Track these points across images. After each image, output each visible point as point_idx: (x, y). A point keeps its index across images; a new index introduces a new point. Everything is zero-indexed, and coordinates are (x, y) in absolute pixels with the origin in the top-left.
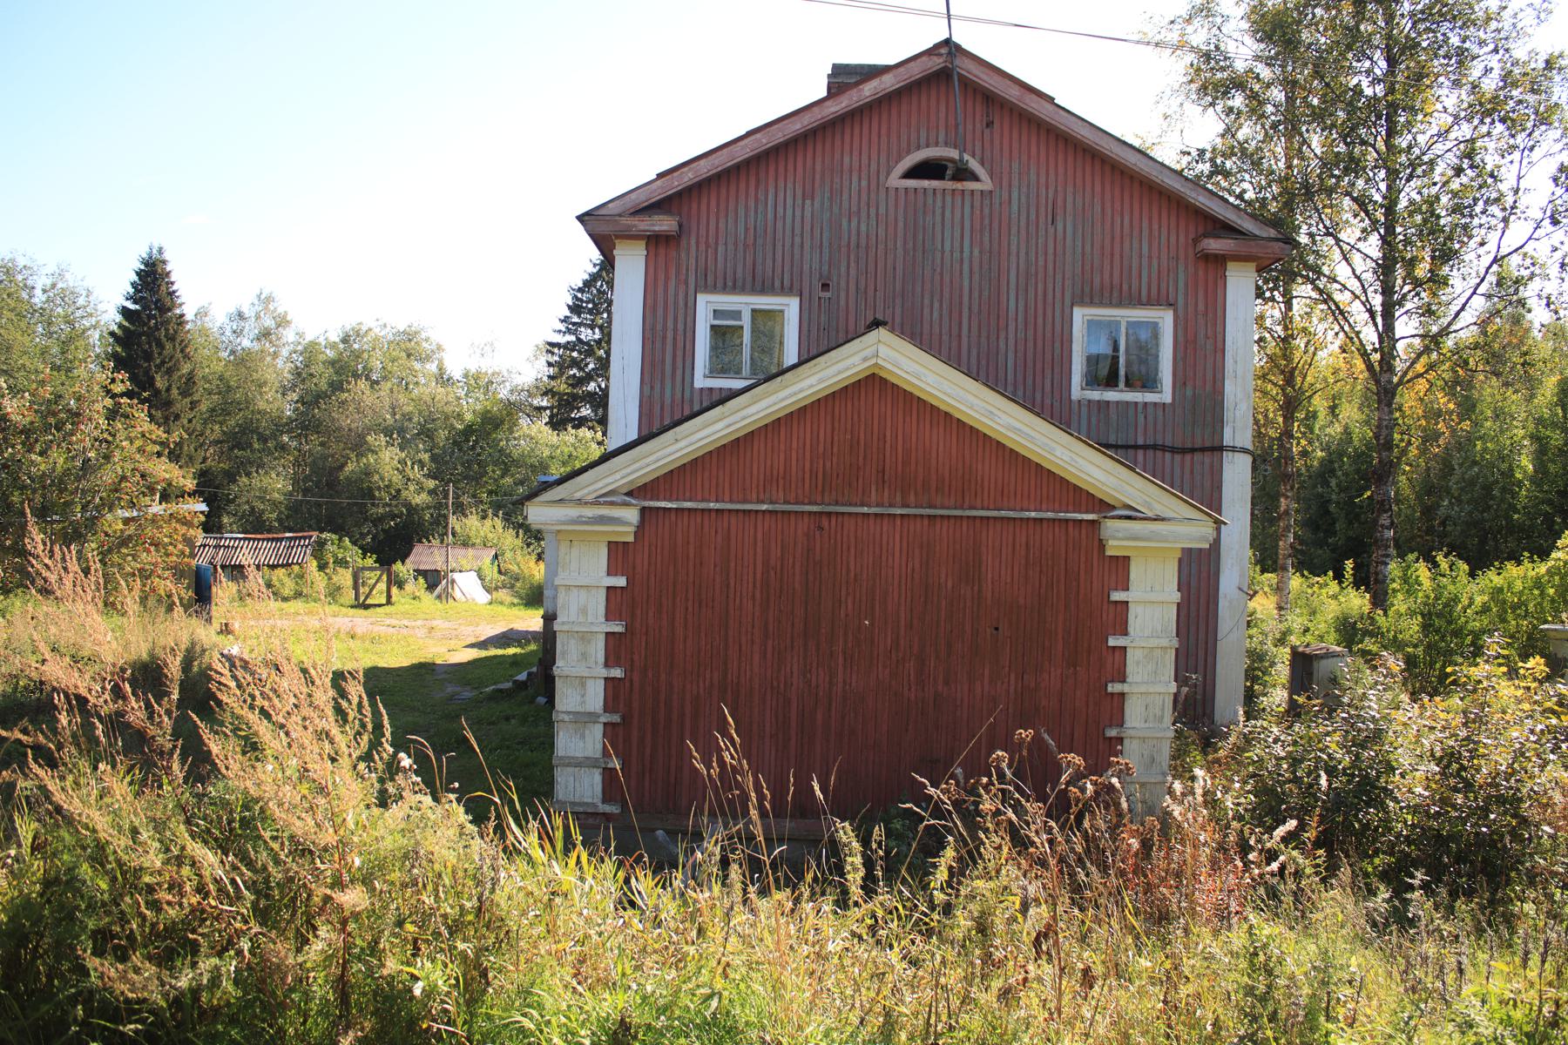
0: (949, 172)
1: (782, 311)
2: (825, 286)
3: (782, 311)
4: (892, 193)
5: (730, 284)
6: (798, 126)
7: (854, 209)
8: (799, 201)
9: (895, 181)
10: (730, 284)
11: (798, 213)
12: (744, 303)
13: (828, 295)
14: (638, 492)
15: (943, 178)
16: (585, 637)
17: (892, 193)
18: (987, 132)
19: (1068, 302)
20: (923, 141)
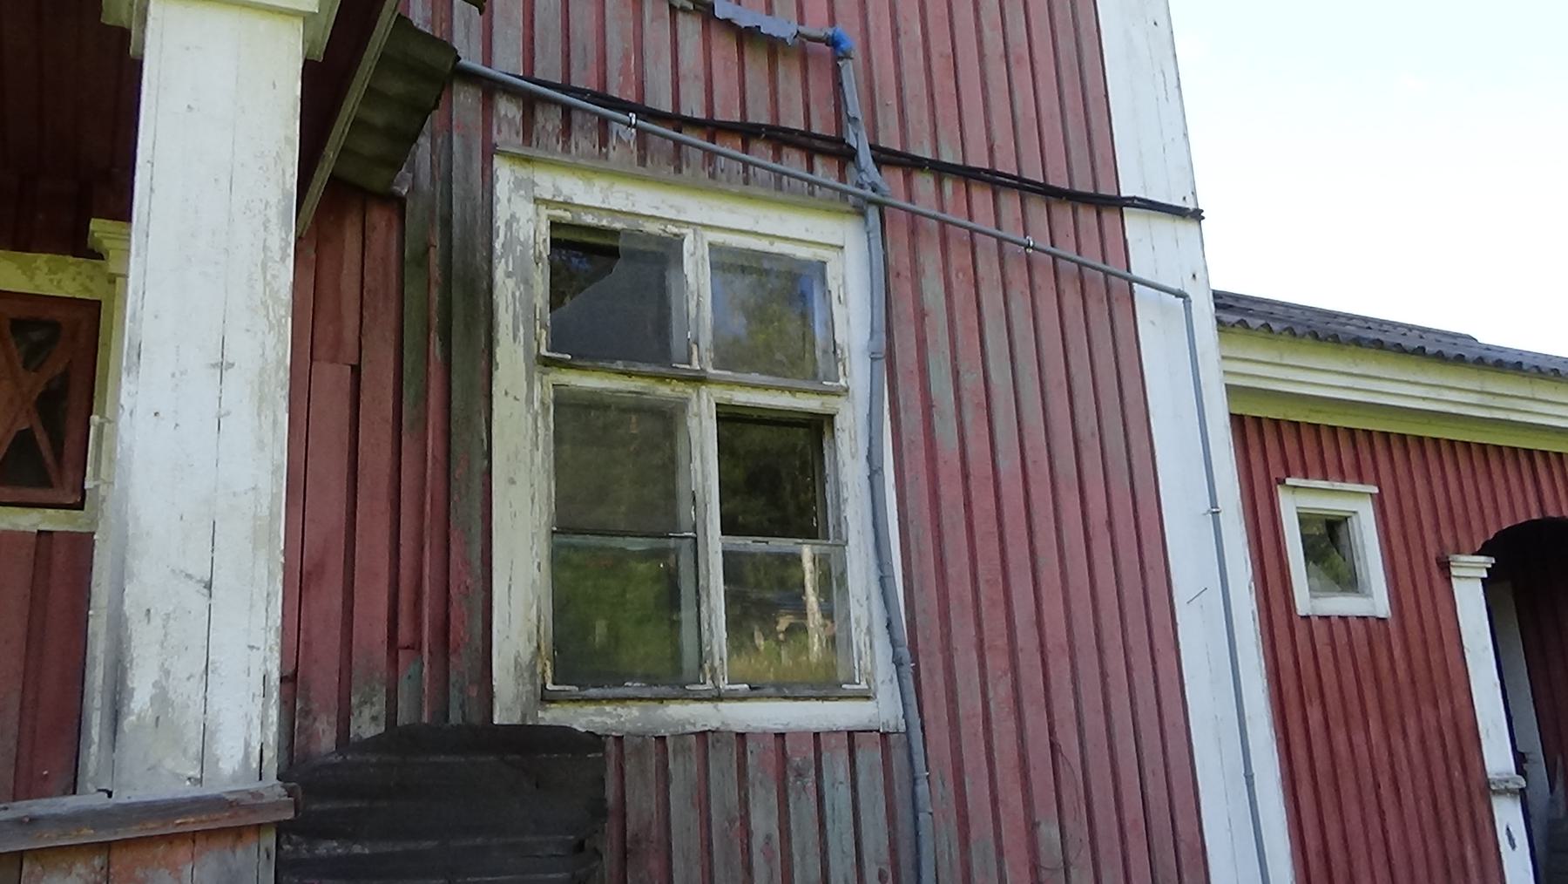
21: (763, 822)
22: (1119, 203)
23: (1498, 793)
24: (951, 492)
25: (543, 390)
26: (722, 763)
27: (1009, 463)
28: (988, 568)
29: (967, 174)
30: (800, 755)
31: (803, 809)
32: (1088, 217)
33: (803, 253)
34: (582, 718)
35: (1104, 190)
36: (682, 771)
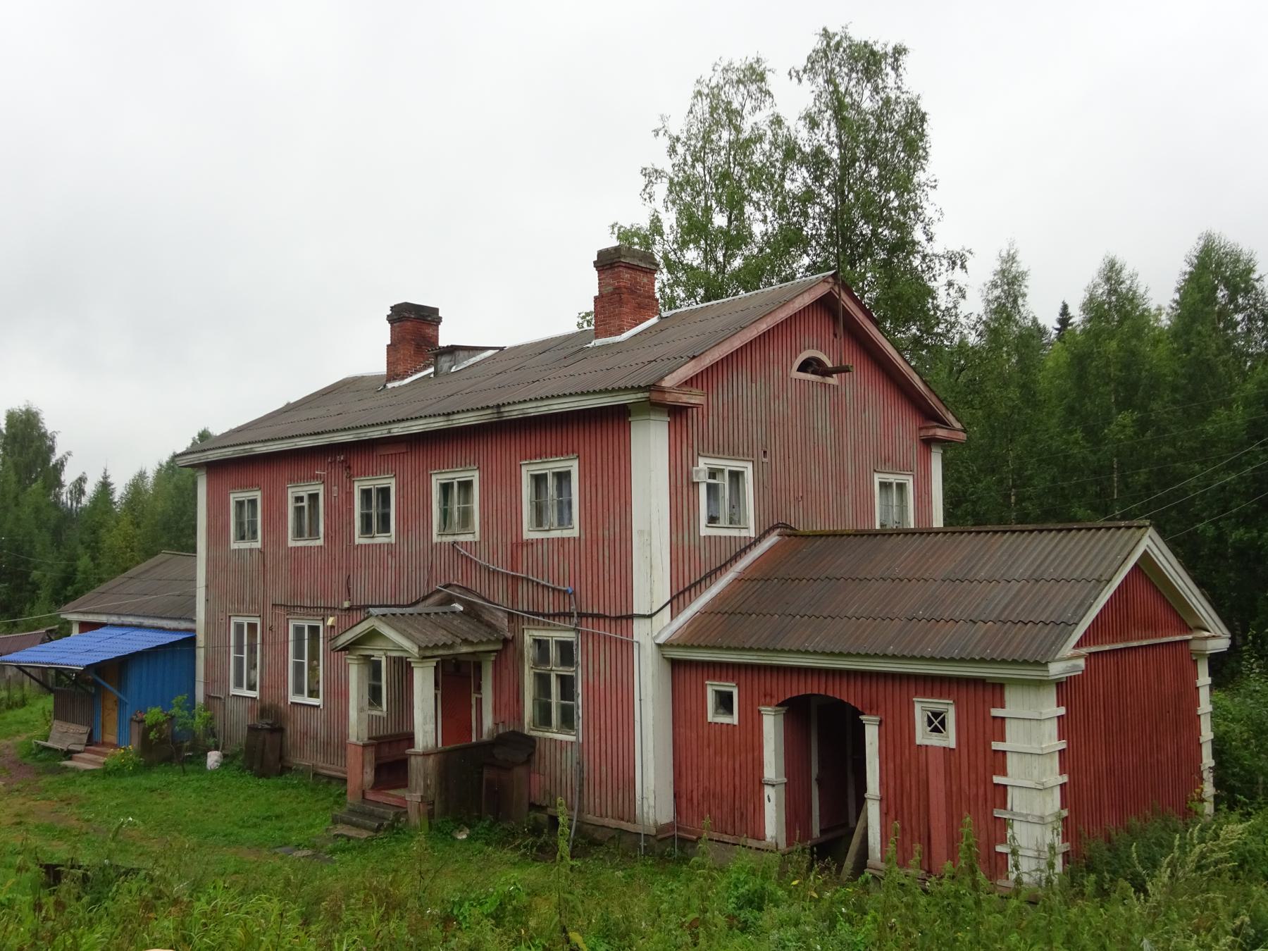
1: (743, 472)
2: (765, 452)
3: (743, 472)
5: (716, 449)
8: (749, 384)
10: (716, 449)
13: (764, 460)
14: (1079, 645)
18: (835, 340)
19: (872, 470)
21: (558, 757)
22: (631, 617)
23: (767, 784)
24: (591, 693)
25: (532, 673)
26: (553, 744)
27: (602, 687)
28: (597, 711)
29: (598, 616)
30: (564, 745)
31: (564, 755)
32: (624, 622)
33: (569, 639)
34: (534, 733)
35: (629, 613)
36: (548, 744)
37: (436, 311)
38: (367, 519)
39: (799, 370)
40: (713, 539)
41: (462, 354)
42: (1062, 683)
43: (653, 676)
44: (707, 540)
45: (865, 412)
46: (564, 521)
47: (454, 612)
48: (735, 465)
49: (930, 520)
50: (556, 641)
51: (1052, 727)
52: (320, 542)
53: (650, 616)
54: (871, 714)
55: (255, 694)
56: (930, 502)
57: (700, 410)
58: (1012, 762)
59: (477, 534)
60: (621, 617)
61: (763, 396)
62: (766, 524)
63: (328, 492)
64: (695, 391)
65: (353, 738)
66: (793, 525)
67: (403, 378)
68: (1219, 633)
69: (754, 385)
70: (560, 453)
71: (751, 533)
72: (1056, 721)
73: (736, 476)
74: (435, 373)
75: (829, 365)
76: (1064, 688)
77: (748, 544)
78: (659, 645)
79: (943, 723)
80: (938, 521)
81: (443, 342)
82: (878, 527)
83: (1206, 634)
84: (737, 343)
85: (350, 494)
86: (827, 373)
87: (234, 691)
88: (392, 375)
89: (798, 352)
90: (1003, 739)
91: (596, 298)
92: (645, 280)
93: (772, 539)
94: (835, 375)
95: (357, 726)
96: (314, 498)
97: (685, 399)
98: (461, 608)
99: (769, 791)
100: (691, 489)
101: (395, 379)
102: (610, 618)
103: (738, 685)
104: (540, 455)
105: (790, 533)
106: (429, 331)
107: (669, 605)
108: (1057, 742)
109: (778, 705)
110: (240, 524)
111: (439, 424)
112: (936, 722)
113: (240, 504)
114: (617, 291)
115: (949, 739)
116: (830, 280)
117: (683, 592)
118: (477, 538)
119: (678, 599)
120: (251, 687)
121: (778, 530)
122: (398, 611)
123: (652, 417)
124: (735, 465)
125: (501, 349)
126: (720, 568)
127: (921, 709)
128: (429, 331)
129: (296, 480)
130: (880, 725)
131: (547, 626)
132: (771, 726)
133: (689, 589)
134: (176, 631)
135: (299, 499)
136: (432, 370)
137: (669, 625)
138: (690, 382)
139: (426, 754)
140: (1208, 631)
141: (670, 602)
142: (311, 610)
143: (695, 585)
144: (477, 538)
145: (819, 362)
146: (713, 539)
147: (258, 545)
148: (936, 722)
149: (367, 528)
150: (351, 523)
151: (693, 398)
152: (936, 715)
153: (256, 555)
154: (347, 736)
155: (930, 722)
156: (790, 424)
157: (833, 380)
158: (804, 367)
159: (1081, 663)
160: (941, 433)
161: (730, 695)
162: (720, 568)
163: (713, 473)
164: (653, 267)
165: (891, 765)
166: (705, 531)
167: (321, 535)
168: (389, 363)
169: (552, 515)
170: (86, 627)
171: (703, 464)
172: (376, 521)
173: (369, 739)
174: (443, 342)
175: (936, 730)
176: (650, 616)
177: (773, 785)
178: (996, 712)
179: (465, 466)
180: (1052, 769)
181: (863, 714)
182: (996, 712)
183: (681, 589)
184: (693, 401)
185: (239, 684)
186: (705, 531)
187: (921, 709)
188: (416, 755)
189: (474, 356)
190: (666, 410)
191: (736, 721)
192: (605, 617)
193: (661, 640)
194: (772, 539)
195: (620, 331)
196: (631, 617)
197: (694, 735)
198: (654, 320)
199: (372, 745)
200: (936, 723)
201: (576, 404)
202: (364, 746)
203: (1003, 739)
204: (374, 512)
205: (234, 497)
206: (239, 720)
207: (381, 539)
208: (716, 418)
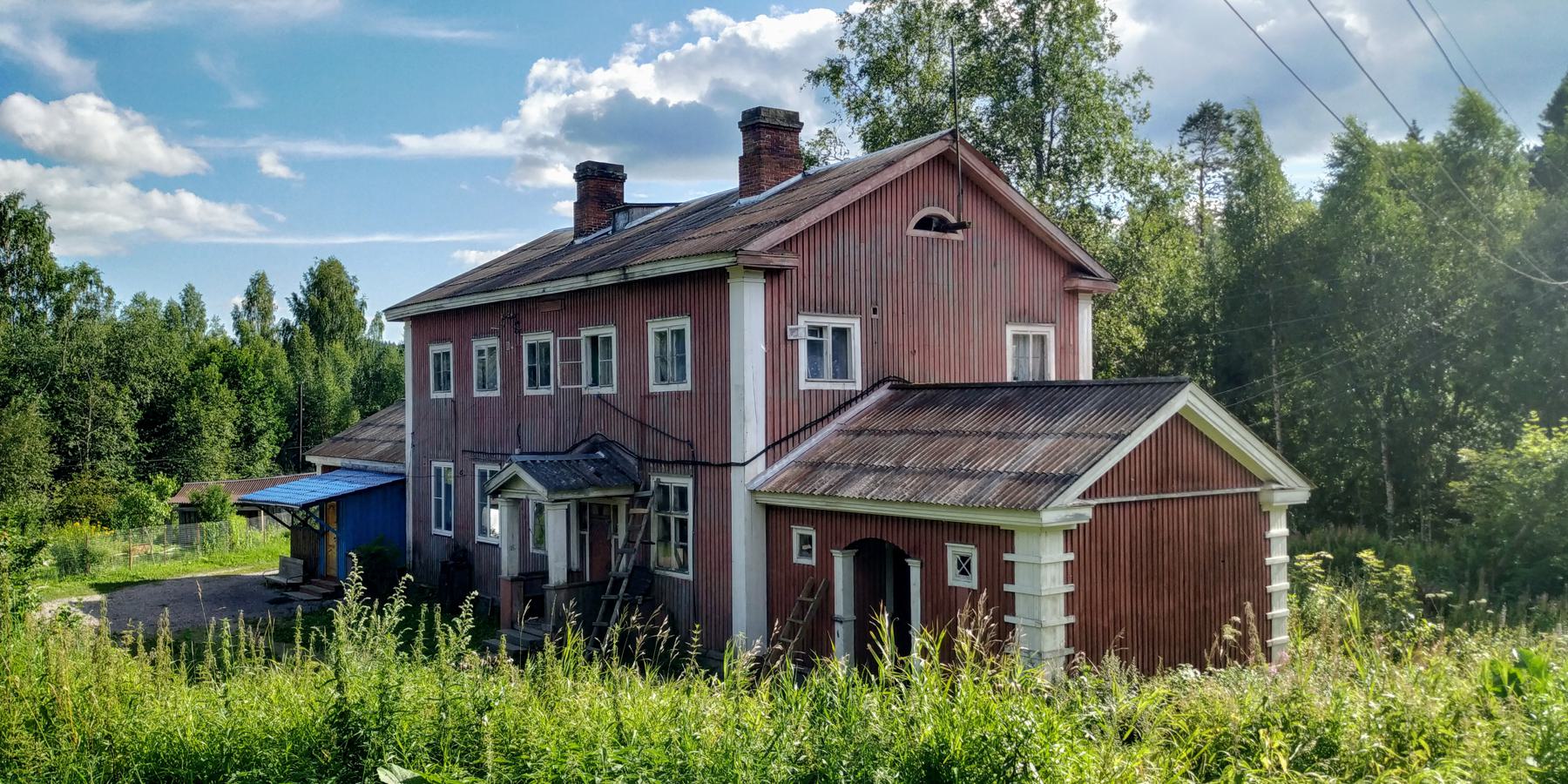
0: (934, 225)
1: (850, 329)
2: (875, 311)
3: (850, 329)
4: (910, 239)
5: (818, 307)
6: (869, 188)
7: (889, 251)
9: (912, 232)
10: (818, 307)
11: (857, 253)
12: (831, 322)
13: (874, 316)
15: (930, 229)
16: (1054, 597)
17: (910, 239)
20: (926, 204)
22: (729, 465)
32: (724, 469)
37: (622, 167)
38: (532, 370)
39: (916, 228)
40: (813, 394)
41: (635, 211)
42: (1072, 531)
43: (746, 520)
44: (807, 394)
45: (995, 265)
46: (682, 378)
47: (595, 460)
48: (840, 322)
49: (1076, 371)
50: (675, 487)
51: (1059, 572)
52: (497, 393)
53: (744, 464)
54: (915, 559)
55: (450, 533)
56: (1076, 353)
57: (794, 272)
58: (1020, 604)
59: (615, 387)
60: (722, 465)
61: (874, 255)
62: (875, 376)
63: (503, 347)
64: (786, 255)
65: (504, 574)
66: (907, 379)
67: (587, 235)
68: (1293, 485)
69: (863, 244)
70: (677, 312)
71: (859, 387)
72: (1062, 566)
73: (841, 334)
74: (614, 231)
75: (953, 220)
76: (1070, 537)
77: (853, 397)
78: (753, 492)
79: (968, 566)
80: (1085, 373)
81: (627, 200)
82: (1009, 379)
83: (1275, 486)
84: (836, 204)
85: (519, 348)
86: (952, 228)
87: (435, 531)
88: (579, 232)
89: (915, 210)
90: (1013, 582)
91: (740, 158)
92: (789, 139)
93: (882, 393)
94: (959, 231)
95: (509, 564)
96: (492, 350)
97: (776, 261)
98: (603, 456)
99: (838, 627)
100: (789, 345)
101: (581, 236)
102: (714, 465)
103: (816, 528)
104: (663, 314)
105: (902, 387)
106: (614, 188)
107: (764, 454)
108: (1062, 585)
109: (846, 548)
110: (437, 376)
111: (578, 283)
112: (964, 566)
113: (437, 356)
114: (758, 151)
115: (972, 582)
116: (949, 137)
117: (780, 442)
118: (615, 392)
119: (775, 447)
120: (448, 527)
121: (889, 383)
122: (555, 458)
123: (745, 280)
124: (840, 322)
125: (676, 205)
126: (822, 420)
127: (954, 551)
128: (614, 188)
129: (478, 335)
130: (921, 567)
131: (667, 473)
132: (841, 566)
133: (786, 439)
134: (392, 474)
135: (481, 352)
136: (610, 228)
137: (763, 473)
138: (785, 246)
139: (557, 588)
140: (1278, 483)
141: (766, 451)
142: (491, 457)
143: (793, 435)
144: (615, 392)
145: (942, 220)
146: (813, 394)
147: (450, 395)
148: (964, 566)
149: (532, 383)
150: (520, 375)
151: (788, 261)
152: (964, 559)
153: (450, 404)
154: (498, 570)
155: (959, 566)
156: (905, 281)
157: (959, 236)
158: (924, 224)
159: (1089, 512)
160: (1084, 284)
161: (810, 537)
162: (822, 420)
163: (816, 331)
164: (796, 126)
165: (929, 605)
166: (804, 385)
167: (499, 387)
168: (576, 220)
169: (671, 371)
170: (327, 469)
171: (804, 321)
172: (540, 376)
173: (519, 574)
174: (627, 200)
175: (963, 573)
176: (744, 464)
177: (841, 622)
178: (1007, 557)
179: (605, 323)
180: (1055, 611)
181: (908, 557)
182: (1007, 557)
183: (777, 439)
184: (786, 264)
185: (439, 525)
186: (804, 385)
187: (954, 551)
188: (550, 589)
189: (648, 213)
190: (762, 272)
191: (814, 564)
192: (709, 464)
193: (752, 487)
194: (882, 393)
195: (759, 190)
196: (729, 465)
197: (783, 577)
198: (799, 176)
199: (521, 580)
200: (964, 565)
201: (681, 267)
202: (513, 580)
203: (1013, 582)
204: (537, 365)
205: (435, 349)
206: (437, 554)
207: (543, 391)
208: (818, 278)
